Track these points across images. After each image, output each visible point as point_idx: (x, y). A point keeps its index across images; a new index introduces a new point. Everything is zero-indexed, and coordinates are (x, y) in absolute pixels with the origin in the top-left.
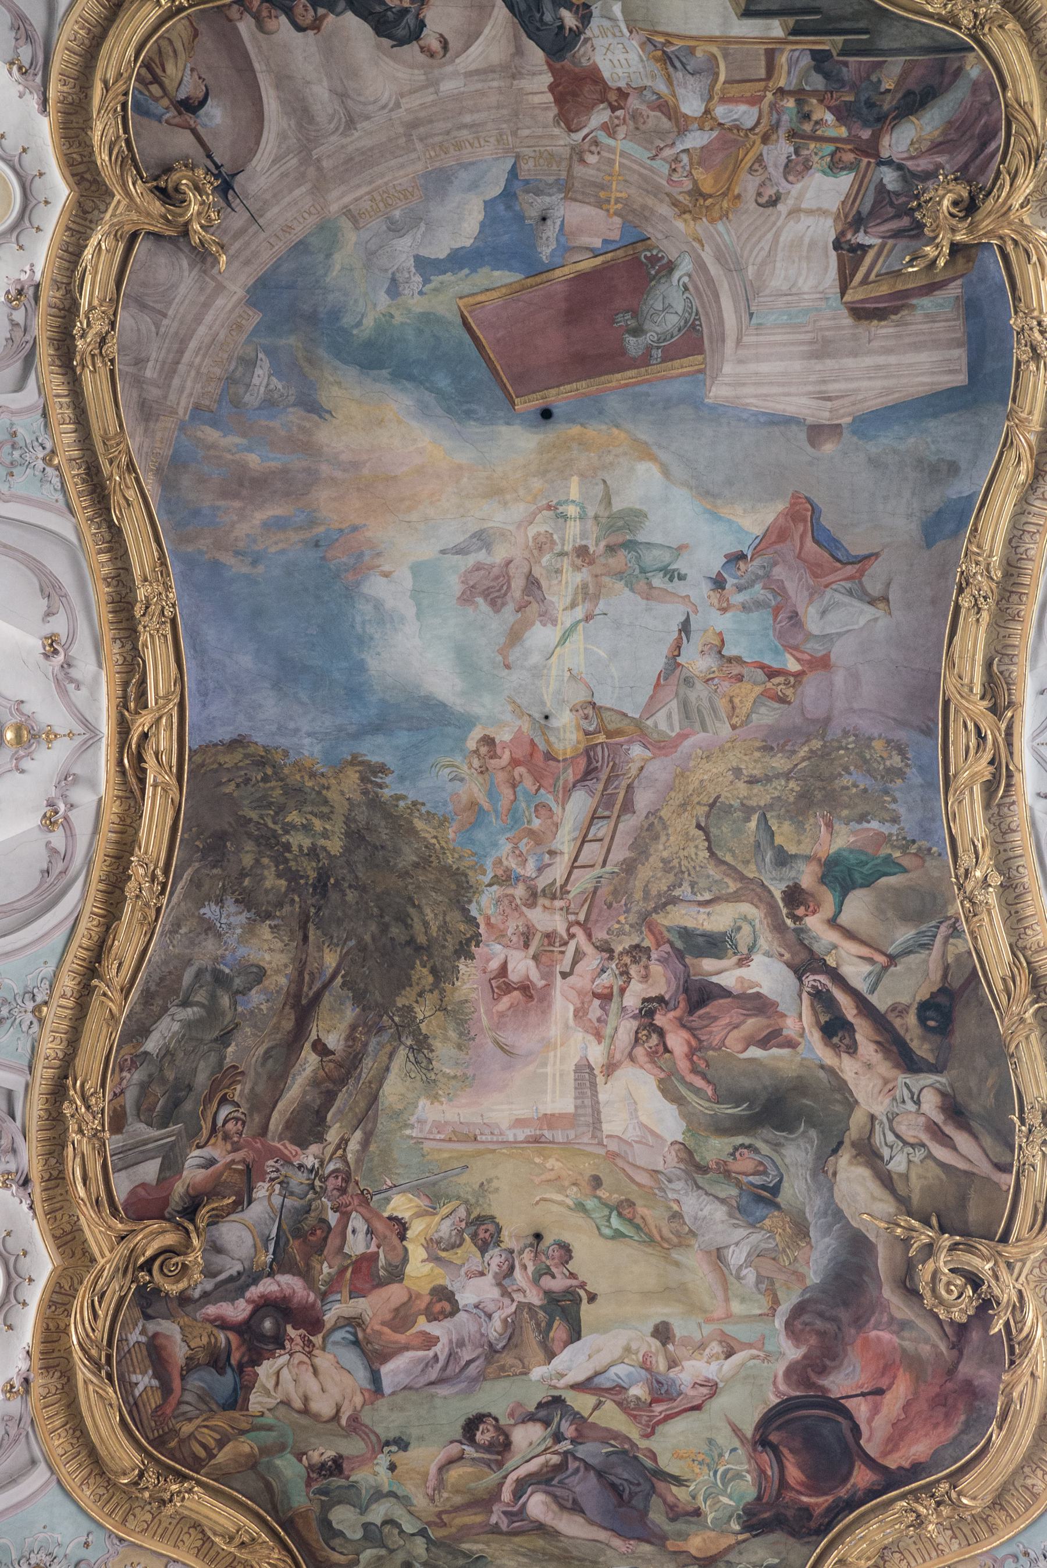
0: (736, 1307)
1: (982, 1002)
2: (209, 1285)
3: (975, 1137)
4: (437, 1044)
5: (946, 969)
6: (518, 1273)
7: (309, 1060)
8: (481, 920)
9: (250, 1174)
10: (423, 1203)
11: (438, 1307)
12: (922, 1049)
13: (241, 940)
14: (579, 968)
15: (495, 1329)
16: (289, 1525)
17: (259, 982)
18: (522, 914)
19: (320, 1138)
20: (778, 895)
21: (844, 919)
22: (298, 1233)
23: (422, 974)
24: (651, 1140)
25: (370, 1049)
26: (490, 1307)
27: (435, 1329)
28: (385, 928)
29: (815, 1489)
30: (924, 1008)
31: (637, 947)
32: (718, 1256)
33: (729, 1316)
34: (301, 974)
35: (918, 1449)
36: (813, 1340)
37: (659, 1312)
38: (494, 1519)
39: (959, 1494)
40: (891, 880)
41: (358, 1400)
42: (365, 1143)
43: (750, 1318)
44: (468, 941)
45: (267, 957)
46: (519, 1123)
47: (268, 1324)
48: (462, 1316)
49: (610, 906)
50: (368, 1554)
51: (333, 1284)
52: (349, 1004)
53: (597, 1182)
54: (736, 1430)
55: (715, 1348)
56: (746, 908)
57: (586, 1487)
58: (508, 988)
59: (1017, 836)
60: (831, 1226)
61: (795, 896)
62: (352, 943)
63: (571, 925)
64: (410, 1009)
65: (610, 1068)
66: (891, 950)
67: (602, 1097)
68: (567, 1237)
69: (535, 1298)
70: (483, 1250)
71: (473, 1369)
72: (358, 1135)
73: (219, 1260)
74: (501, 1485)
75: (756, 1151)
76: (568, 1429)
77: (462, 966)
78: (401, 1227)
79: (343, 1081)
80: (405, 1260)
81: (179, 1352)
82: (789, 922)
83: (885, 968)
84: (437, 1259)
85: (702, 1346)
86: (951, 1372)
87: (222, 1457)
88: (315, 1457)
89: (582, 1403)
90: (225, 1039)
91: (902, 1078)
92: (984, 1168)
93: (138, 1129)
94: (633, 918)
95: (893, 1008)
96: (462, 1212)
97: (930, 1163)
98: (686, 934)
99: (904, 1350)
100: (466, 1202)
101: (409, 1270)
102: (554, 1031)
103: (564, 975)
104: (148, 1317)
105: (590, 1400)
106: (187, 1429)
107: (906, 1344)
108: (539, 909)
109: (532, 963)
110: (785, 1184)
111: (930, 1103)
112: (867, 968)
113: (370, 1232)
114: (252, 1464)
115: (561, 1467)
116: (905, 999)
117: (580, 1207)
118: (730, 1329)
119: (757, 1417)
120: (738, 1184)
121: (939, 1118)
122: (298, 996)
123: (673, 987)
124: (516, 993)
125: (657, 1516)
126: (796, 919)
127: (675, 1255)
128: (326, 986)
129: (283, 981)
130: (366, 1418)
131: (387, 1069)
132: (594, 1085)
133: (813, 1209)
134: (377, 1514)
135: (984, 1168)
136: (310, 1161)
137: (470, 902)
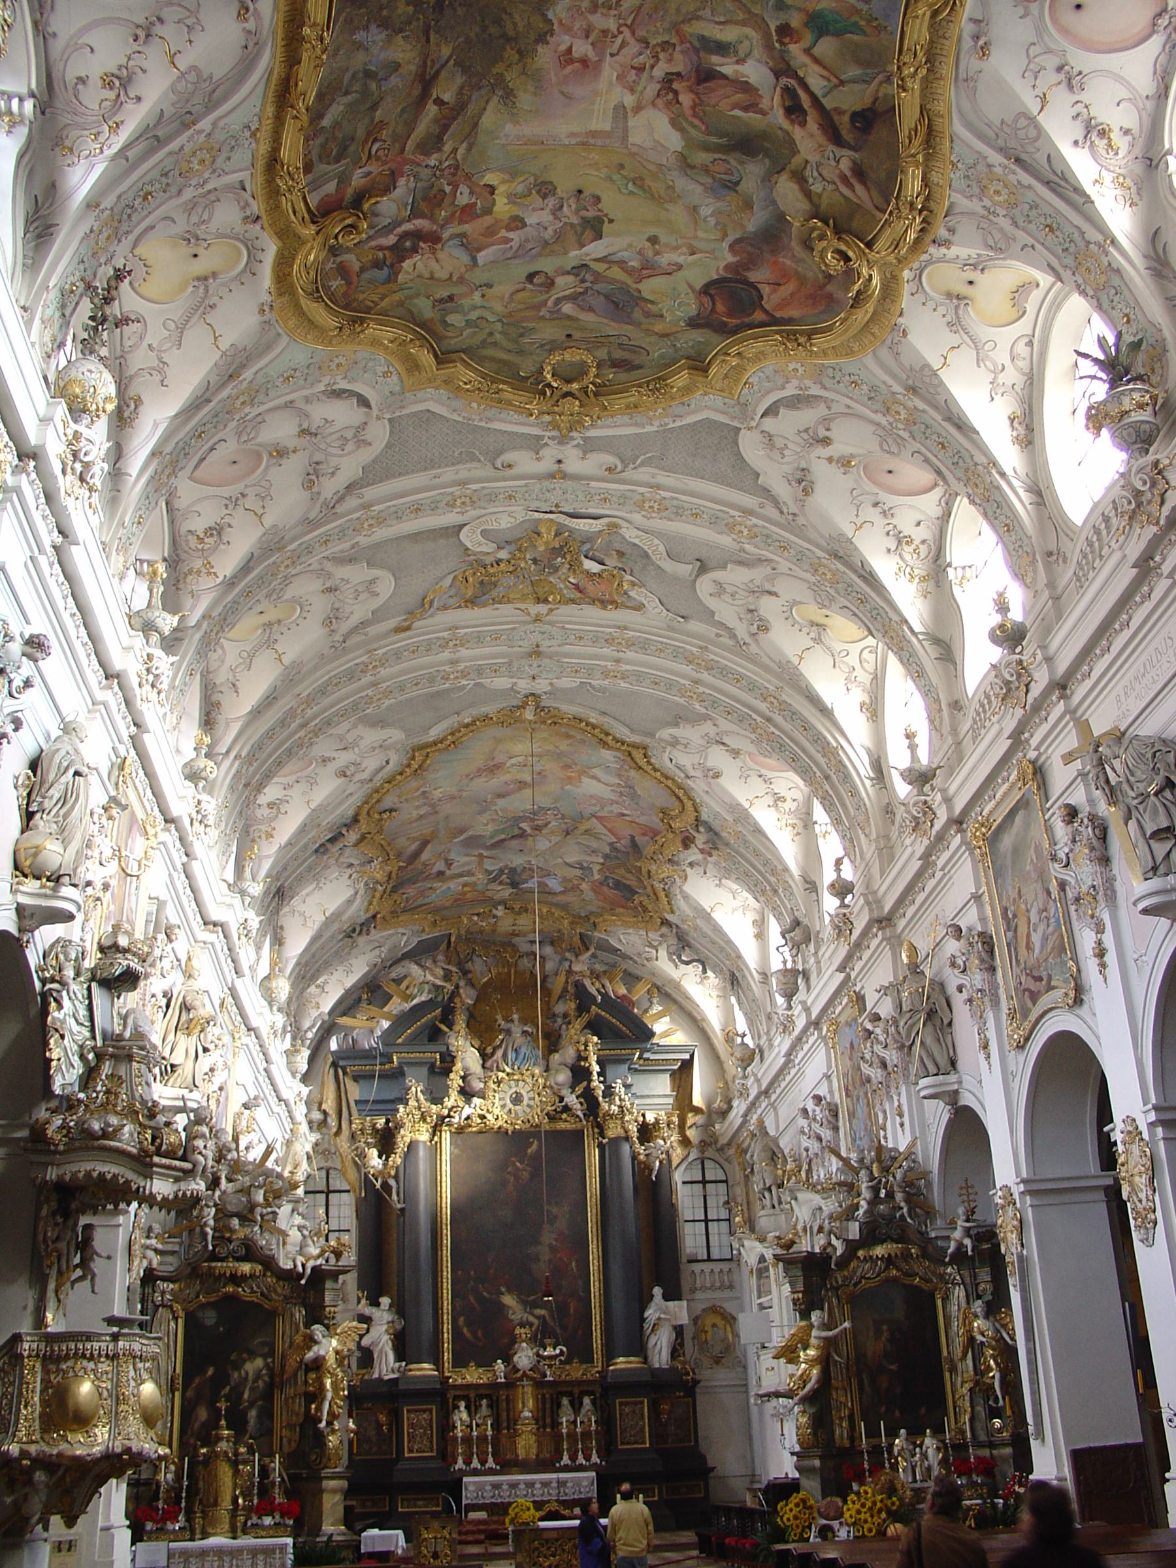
0: (700, 234)
1: (894, 124)
2: (371, 232)
3: (868, 189)
4: (520, 94)
5: (876, 99)
6: (565, 208)
7: (432, 110)
8: (555, 22)
9: (394, 176)
10: (506, 177)
11: (513, 225)
12: (846, 134)
13: (382, 49)
14: (623, 52)
15: (548, 234)
16: (423, 325)
17: (397, 70)
18: (586, 18)
19: (439, 150)
20: (773, 28)
21: (816, 51)
22: (424, 199)
23: (511, 54)
24: (659, 148)
25: (474, 98)
26: (547, 224)
27: (511, 235)
28: (485, 29)
29: (729, 316)
30: (855, 116)
31: (667, 42)
32: (695, 209)
33: (695, 237)
34: (425, 62)
35: (795, 313)
36: (745, 255)
37: (652, 231)
38: (542, 314)
39: (811, 345)
40: (855, 37)
41: (463, 270)
42: (469, 149)
43: (707, 240)
44: (545, 34)
45: (401, 55)
46: (572, 135)
47: (408, 244)
48: (528, 228)
49: (650, 16)
50: (468, 331)
51: (448, 221)
52: (459, 75)
53: (622, 166)
54: (690, 287)
55: (684, 250)
56: (748, 31)
57: (598, 302)
58: (571, 61)
59: (947, 43)
60: (767, 207)
61: (785, 31)
62: (461, 39)
63: (620, 26)
64: (502, 75)
65: (638, 109)
66: (843, 77)
67: (631, 124)
68: (598, 193)
69: (575, 220)
70: (544, 197)
71: (534, 251)
72: (464, 145)
73: (376, 220)
74: (546, 301)
75: (728, 163)
76: (588, 277)
77: (540, 49)
78: (492, 189)
79: (455, 118)
80: (494, 204)
81: (356, 266)
82: (777, 45)
83: (836, 86)
84: (514, 203)
85: (676, 248)
86: (822, 287)
87: (383, 304)
88: (438, 296)
89: (600, 267)
90: (374, 107)
91: (831, 147)
92: (869, 205)
93: (322, 168)
94: (666, 25)
95: (835, 109)
96: (532, 180)
97: (837, 194)
98: (702, 39)
99: (797, 272)
100: (535, 175)
101: (495, 209)
102: (602, 85)
103: (612, 55)
104: (336, 256)
105: (606, 266)
106: (361, 297)
107: (800, 269)
108: (598, 15)
109: (590, 47)
110: (743, 183)
111: (845, 165)
112: (825, 83)
113: (471, 193)
114: (401, 304)
115: (585, 292)
116: (844, 107)
117: (610, 179)
118: (694, 243)
119: (704, 282)
120: (713, 178)
121: (848, 174)
122: (423, 75)
123: (689, 68)
124: (577, 64)
125: (637, 314)
126: (782, 43)
127: (666, 205)
128: (442, 66)
129: (413, 68)
130: (468, 276)
131: (485, 109)
132: (625, 117)
133: (757, 198)
134: (474, 315)
135: (869, 205)
136: (432, 162)
137: (548, 9)
